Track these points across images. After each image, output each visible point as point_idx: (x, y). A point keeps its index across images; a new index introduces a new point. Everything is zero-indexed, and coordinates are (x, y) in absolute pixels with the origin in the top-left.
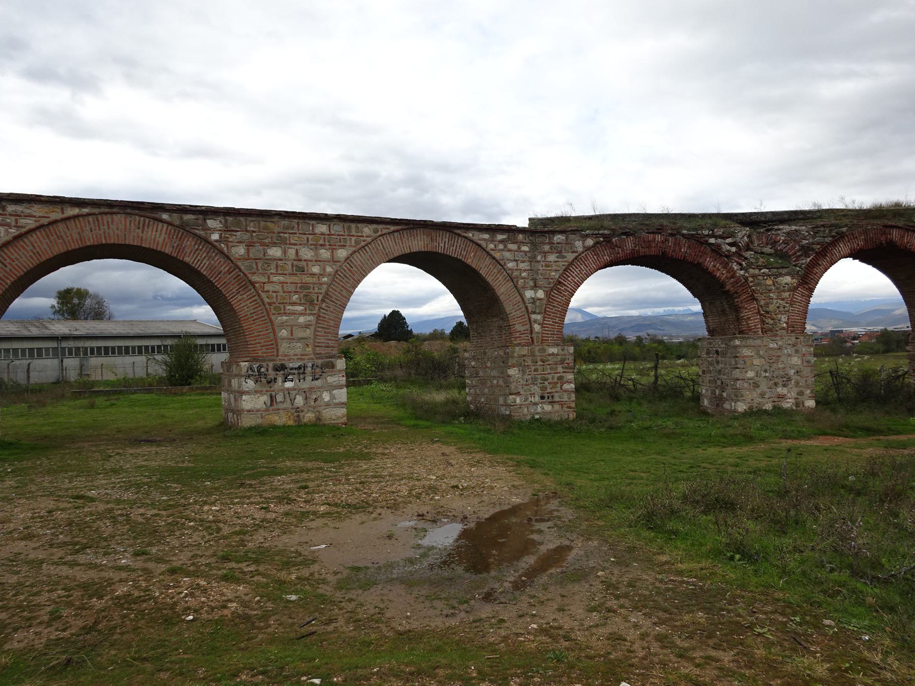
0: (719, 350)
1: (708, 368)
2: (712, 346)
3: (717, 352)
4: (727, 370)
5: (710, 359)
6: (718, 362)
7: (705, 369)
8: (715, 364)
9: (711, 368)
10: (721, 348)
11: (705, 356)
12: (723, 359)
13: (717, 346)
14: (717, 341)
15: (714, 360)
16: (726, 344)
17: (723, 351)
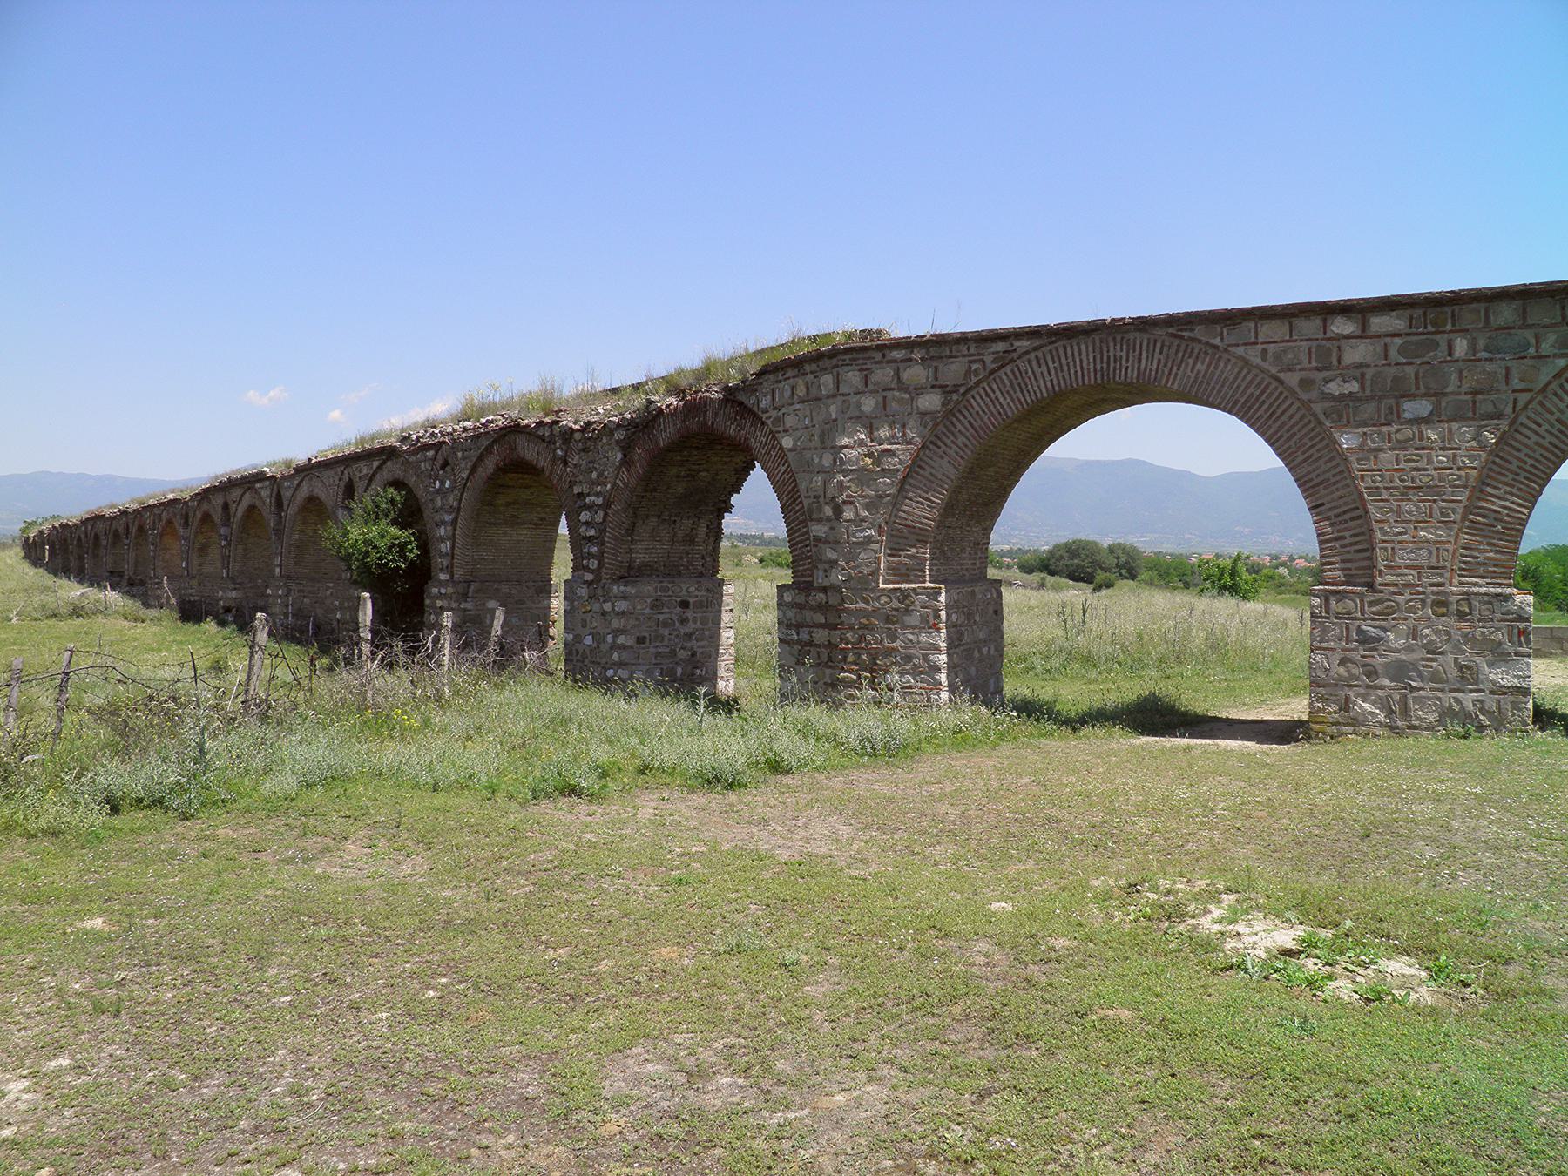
0: (691, 600)
1: (656, 631)
2: (670, 593)
3: (685, 604)
4: (707, 633)
5: (661, 617)
6: (684, 621)
7: (647, 635)
8: (677, 624)
9: (666, 632)
10: (697, 596)
11: (647, 611)
12: (699, 615)
13: (684, 592)
14: (684, 587)
15: (675, 618)
16: (708, 590)
17: (701, 602)
